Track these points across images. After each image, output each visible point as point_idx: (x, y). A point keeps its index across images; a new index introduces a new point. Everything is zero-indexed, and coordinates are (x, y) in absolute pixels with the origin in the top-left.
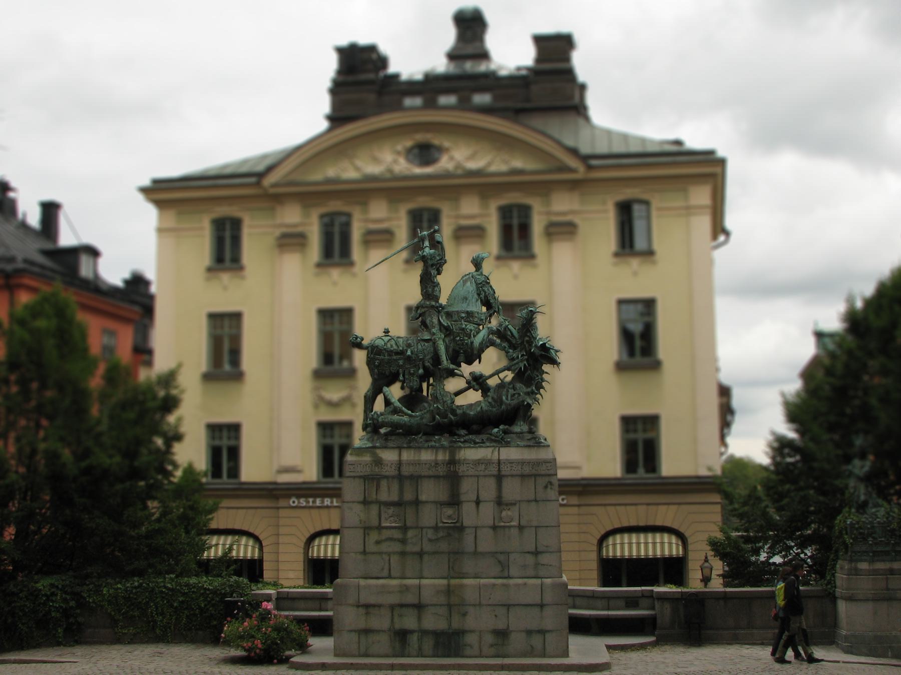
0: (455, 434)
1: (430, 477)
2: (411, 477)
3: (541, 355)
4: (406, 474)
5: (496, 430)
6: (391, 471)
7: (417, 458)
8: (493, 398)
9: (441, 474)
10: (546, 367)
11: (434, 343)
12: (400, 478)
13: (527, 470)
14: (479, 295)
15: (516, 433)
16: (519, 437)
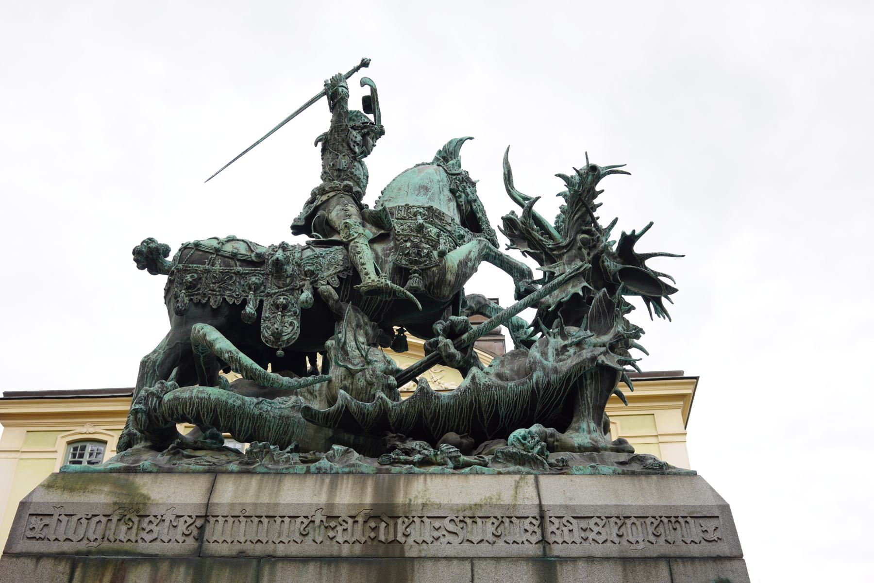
0: (393, 448)
1: (305, 560)
2: (239, 560)
3: (622, 272)
4: (224, 549)
5: (520, 432)
6: (172, 540)
7: (265, 499)
8: (500, 376)
9: (345, 550)
10: (638, 312)
11: (346, 245)
12: (199, 561)
13: (638, 540)
14: (453, 192)
15: (581, 449)
16: (593, 460)
